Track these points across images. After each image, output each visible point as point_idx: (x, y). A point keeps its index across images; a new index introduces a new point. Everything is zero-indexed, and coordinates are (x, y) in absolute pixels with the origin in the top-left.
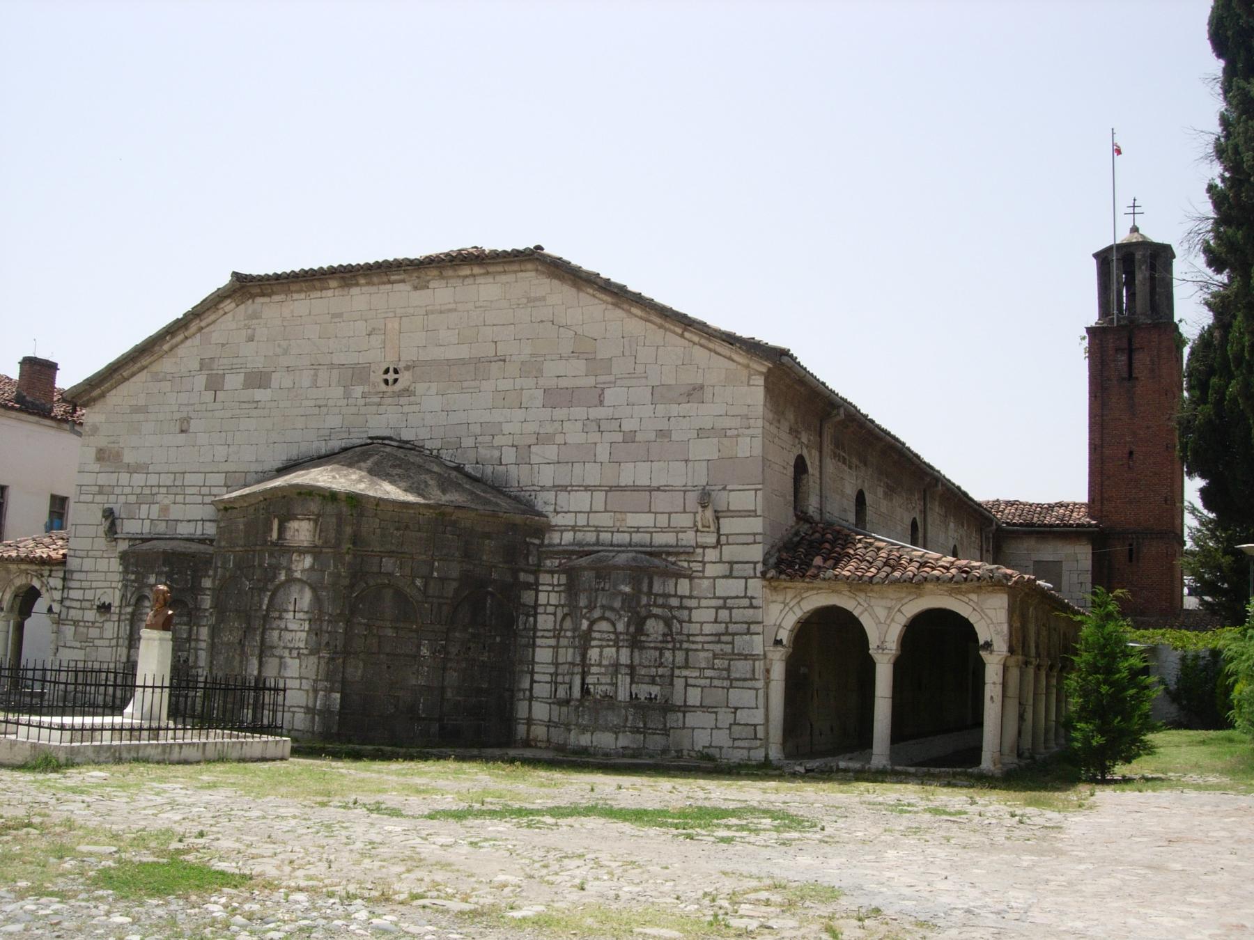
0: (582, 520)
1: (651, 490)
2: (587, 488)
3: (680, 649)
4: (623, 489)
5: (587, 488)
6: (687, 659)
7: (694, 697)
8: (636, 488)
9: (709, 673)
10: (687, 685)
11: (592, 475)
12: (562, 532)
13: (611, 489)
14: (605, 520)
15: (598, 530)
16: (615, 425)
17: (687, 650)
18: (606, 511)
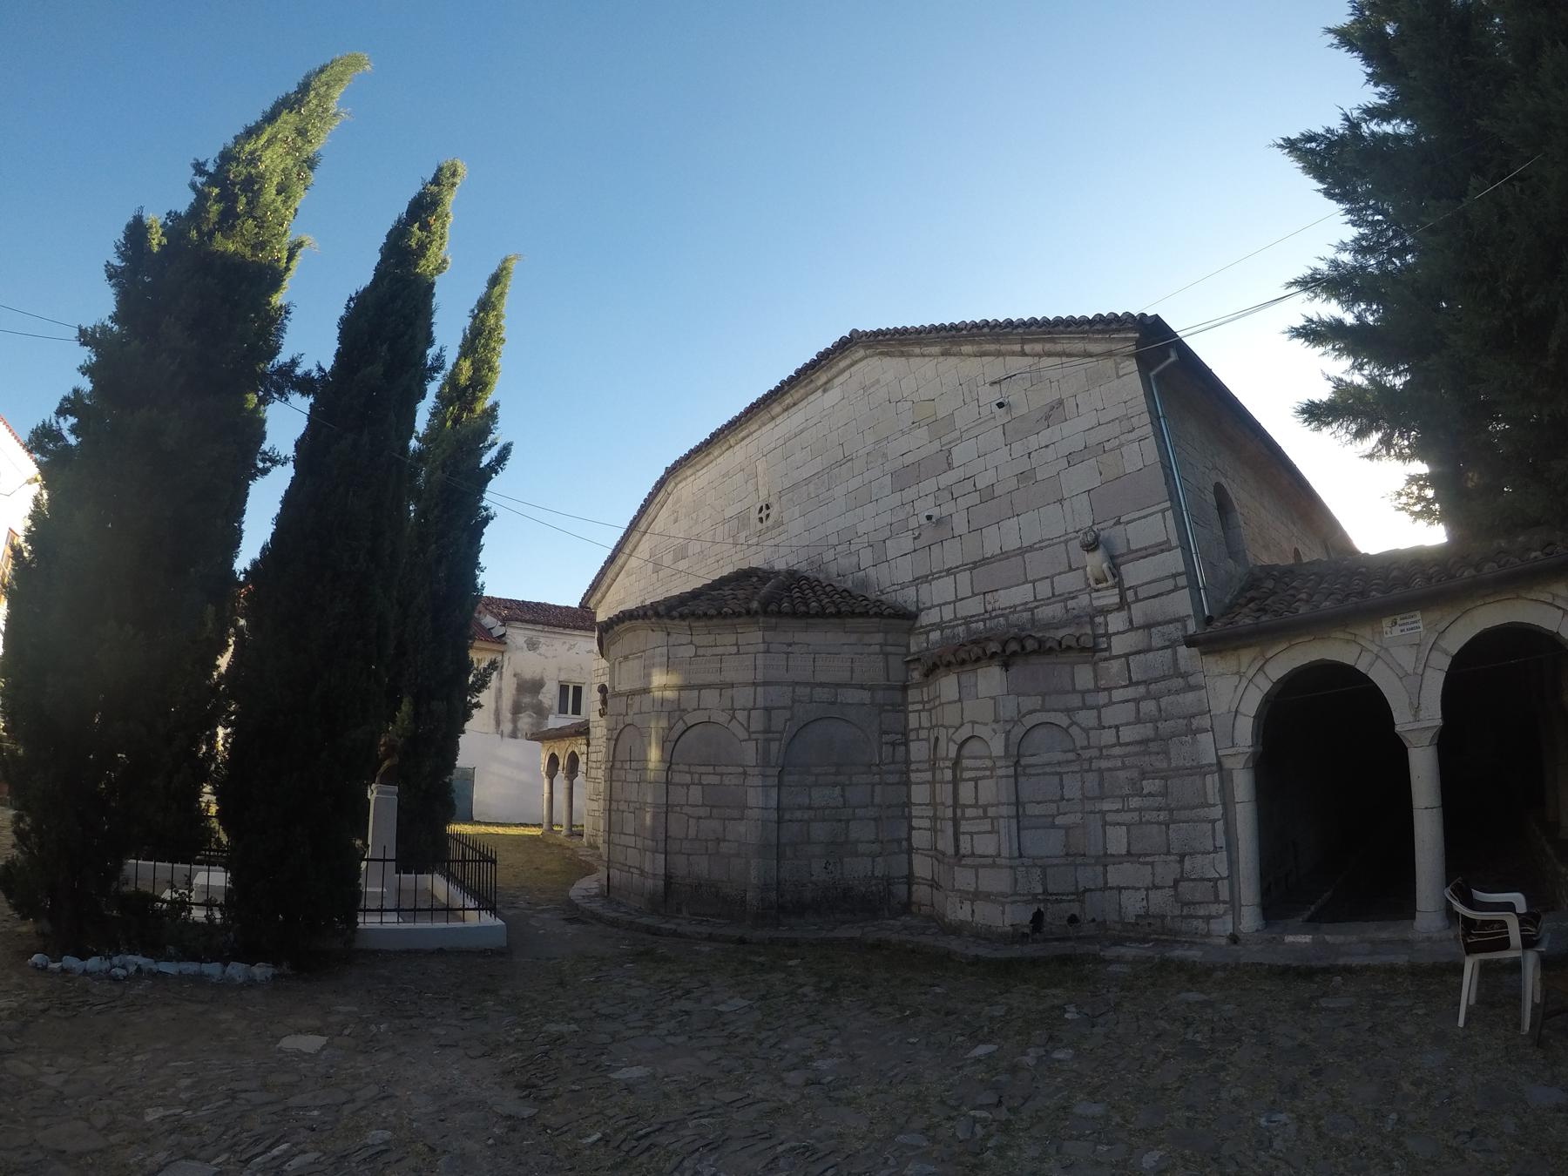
0: (948, 613)
1: (1022, 551)
4: (984, 561)
6: (1101, 785)
7: (1117, 841)
8: (1005, 555)
9: (1135, 802)
10: (1105, 824)
11: (952, 554)
12: (927, 633)
13: (975, 565)
14: (973, 607)
15: (967, 621)
16: (968, 485)
17: (1100, 771)
18: (974, 595)
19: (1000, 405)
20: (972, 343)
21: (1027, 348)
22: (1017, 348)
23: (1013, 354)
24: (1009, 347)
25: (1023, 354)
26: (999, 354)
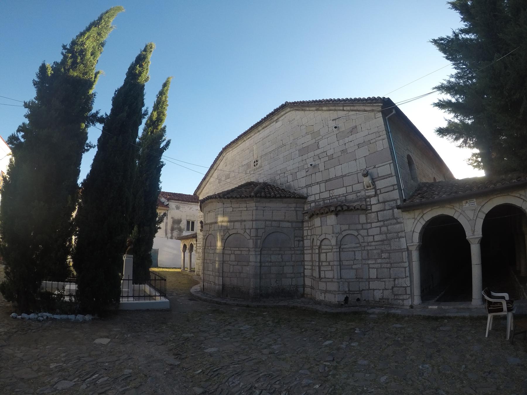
0: (317, 197)
1: (342, 176)
2: (318, 183)
3: (364, 250)
4: (330, 180)
5: (318, 183)
6: (368, 254)
7: (373, 274)
8: (336, 178)
9: (379, 261)
10: (369, 268)
11: (319, 177)
13: (327, 181)
14: (326, 195)
15: (324, 200)
16: (325, 154)
17: (368, 250)
18: (326, 191)
19: (336, 127)
20: (326, 106)
21: (345, 108)
22: (341, 108)
23: (340, 110)
24: (339, 108)
25: (343, 110)
26: (335, 110)
